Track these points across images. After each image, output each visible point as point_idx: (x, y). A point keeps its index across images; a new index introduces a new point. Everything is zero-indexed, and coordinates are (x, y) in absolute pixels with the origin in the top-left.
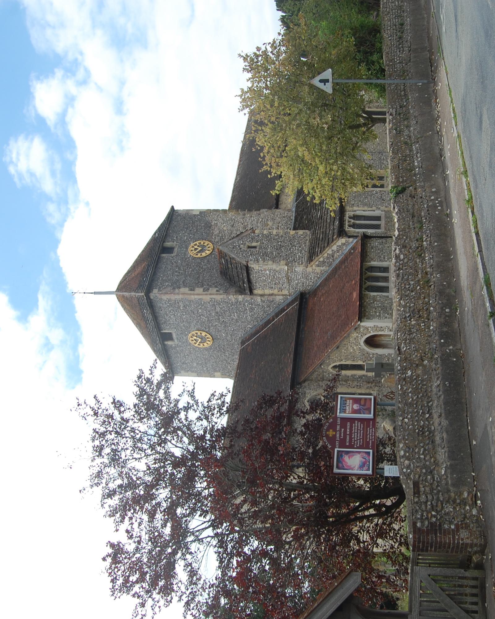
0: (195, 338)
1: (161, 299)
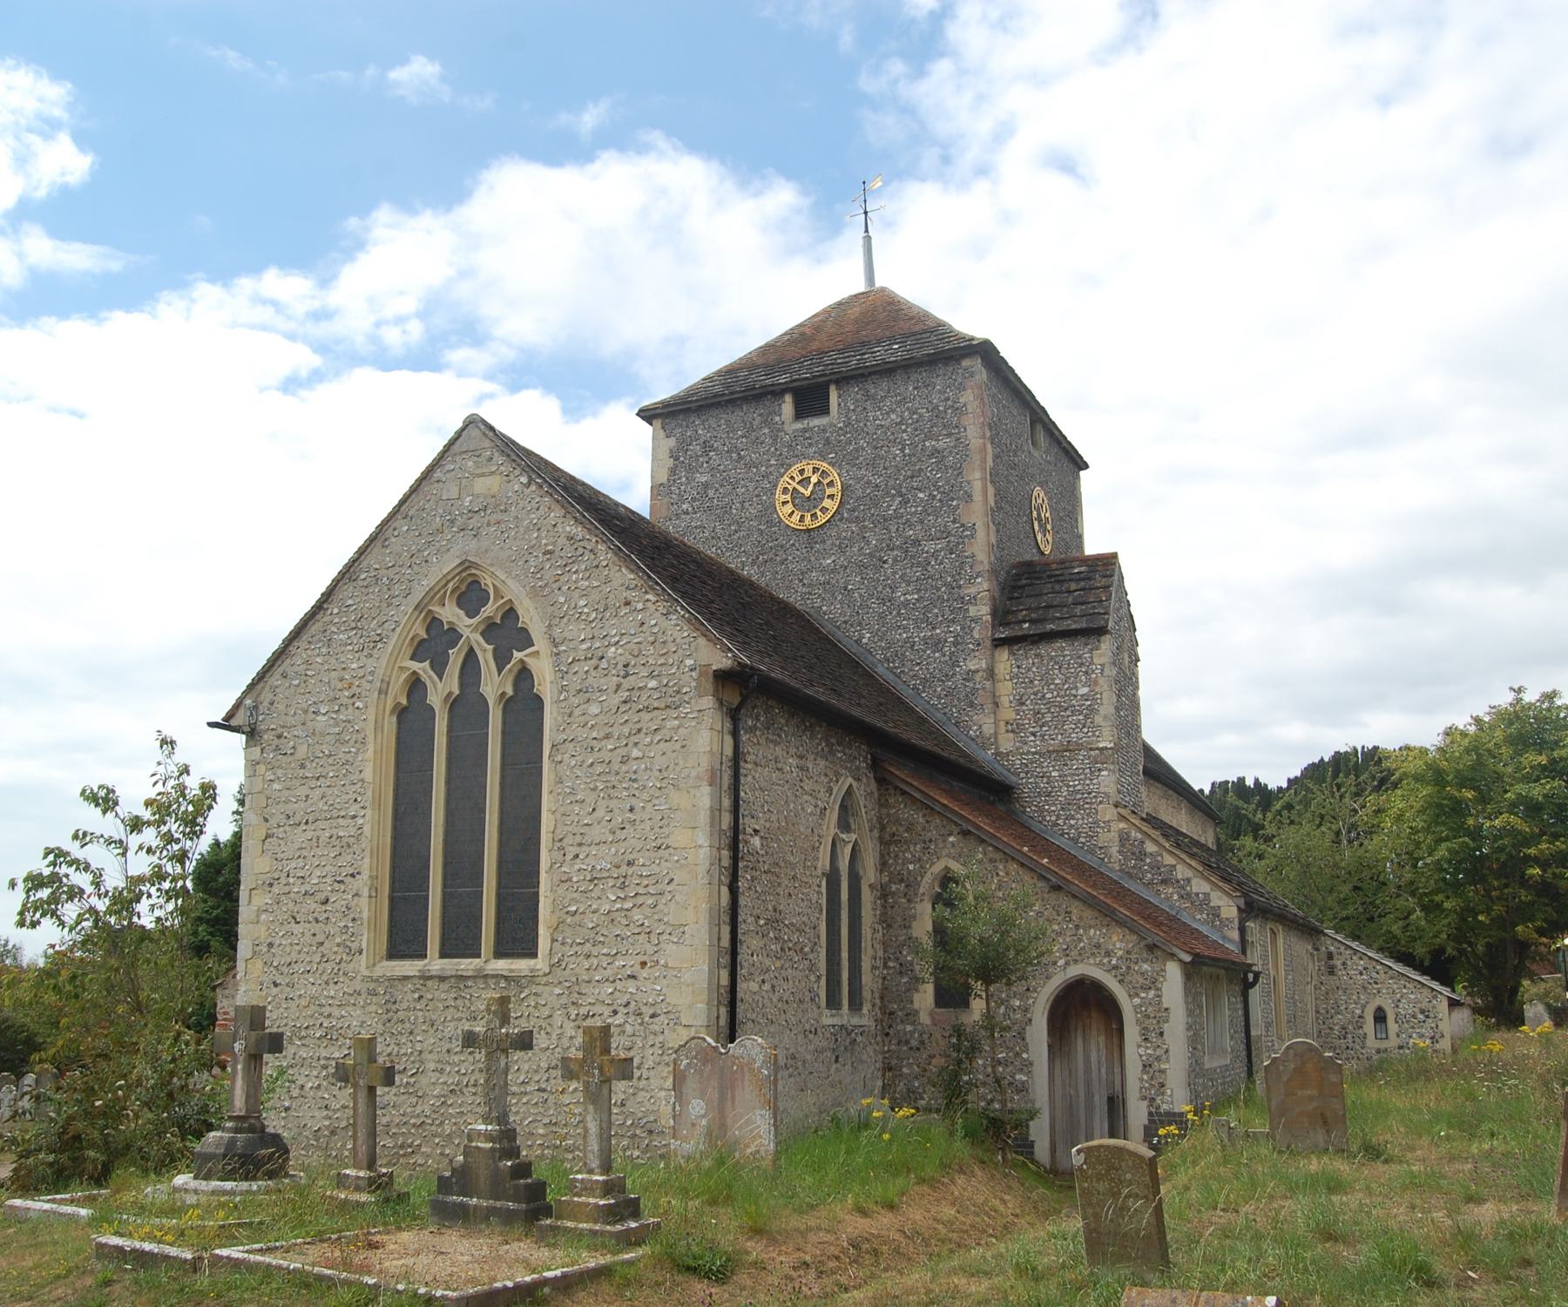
0: (814, 479)
1: (962, 388)
